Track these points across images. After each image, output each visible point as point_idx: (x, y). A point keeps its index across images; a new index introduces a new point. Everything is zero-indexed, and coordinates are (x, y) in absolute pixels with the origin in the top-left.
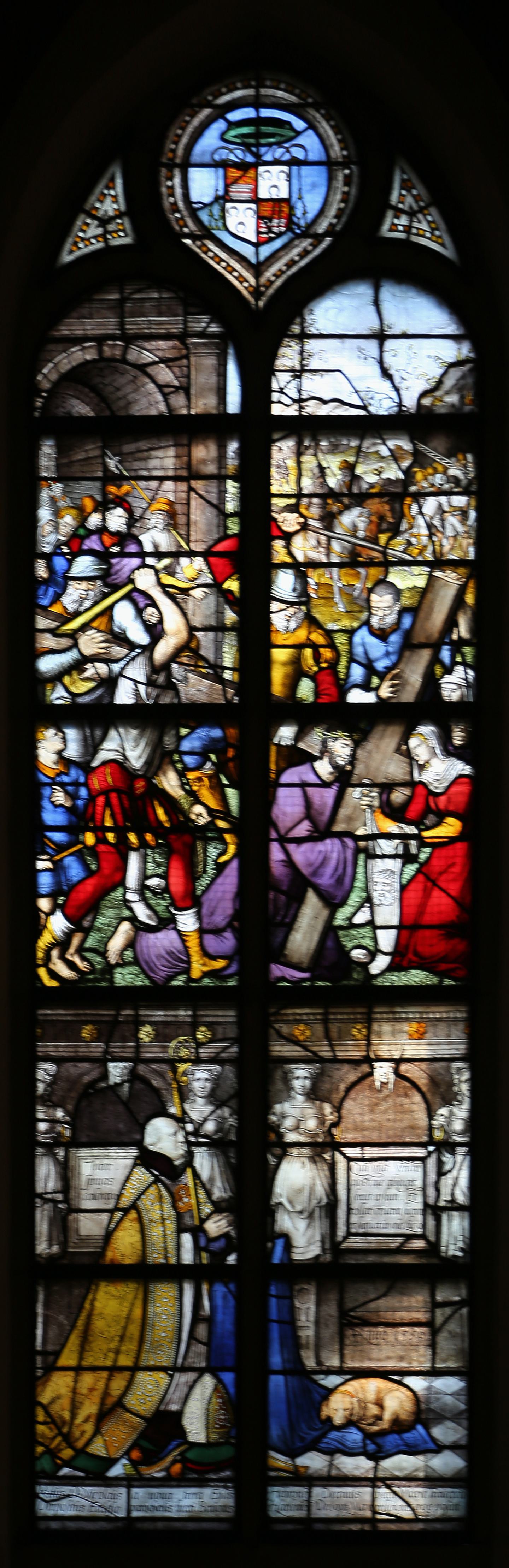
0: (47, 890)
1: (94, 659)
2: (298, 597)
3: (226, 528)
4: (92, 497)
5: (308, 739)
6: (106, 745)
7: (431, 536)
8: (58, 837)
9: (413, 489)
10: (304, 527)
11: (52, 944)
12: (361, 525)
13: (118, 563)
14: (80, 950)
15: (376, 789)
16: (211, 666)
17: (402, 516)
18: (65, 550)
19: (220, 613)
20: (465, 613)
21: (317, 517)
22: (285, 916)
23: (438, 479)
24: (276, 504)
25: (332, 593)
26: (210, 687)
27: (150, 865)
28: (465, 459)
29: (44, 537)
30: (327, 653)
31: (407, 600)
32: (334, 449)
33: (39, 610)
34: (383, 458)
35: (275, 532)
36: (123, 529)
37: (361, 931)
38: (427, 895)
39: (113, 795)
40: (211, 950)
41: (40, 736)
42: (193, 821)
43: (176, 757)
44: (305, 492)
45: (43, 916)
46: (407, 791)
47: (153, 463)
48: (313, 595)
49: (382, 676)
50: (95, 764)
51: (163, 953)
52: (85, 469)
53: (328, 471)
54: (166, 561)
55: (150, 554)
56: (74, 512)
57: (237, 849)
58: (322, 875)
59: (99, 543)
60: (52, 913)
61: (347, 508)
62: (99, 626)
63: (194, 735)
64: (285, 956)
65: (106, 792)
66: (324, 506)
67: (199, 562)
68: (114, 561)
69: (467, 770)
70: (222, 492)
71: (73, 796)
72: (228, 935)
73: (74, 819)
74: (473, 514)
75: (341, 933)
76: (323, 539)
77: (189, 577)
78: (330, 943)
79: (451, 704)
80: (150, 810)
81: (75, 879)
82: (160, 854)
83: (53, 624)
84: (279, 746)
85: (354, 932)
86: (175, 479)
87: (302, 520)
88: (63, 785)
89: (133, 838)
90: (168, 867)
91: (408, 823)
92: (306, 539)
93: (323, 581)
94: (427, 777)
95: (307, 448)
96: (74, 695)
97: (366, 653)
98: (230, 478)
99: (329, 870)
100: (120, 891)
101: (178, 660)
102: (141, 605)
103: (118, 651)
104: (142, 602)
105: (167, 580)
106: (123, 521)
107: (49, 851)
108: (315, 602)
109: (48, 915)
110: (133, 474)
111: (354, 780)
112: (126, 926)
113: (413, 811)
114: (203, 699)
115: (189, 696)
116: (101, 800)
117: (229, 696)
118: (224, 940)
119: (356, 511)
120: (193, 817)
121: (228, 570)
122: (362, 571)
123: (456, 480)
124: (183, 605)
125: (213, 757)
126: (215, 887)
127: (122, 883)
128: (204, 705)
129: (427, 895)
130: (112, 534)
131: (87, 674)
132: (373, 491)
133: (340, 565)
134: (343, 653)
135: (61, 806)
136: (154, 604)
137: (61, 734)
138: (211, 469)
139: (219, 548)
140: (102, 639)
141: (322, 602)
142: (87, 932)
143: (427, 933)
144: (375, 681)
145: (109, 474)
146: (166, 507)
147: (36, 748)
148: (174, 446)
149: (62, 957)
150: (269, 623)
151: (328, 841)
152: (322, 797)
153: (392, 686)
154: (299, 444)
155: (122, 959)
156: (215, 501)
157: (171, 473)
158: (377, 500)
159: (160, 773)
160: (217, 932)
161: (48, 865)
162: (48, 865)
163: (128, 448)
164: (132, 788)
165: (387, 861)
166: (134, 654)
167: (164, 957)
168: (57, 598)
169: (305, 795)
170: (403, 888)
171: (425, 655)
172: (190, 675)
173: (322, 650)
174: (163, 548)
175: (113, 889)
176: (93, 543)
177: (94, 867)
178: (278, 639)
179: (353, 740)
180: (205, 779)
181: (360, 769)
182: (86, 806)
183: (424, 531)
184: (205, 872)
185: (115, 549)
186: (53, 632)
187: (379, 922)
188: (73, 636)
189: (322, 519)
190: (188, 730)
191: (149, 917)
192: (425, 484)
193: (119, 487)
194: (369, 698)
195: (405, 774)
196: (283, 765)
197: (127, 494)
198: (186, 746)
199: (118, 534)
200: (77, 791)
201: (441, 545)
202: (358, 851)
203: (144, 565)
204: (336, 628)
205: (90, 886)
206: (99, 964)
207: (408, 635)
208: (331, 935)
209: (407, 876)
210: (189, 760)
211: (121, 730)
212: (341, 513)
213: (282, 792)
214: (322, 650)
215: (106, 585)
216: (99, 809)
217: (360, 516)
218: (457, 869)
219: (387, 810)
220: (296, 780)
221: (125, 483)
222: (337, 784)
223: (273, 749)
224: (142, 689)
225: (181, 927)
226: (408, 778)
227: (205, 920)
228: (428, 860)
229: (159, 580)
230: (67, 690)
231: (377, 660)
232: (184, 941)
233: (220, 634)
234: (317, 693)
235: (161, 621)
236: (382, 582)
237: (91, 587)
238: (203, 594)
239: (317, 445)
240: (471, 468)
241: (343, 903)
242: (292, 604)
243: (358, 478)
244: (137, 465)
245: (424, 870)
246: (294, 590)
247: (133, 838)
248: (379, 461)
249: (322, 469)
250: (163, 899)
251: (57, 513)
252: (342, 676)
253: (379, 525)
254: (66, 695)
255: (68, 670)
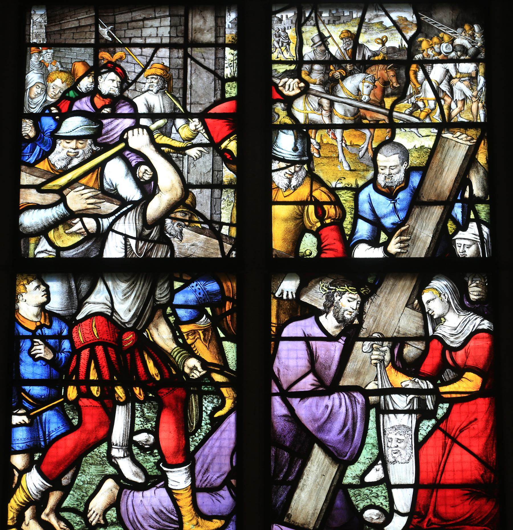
0: (21, 445)
1: (81, 215)
2: (299, 156)
3: (223, 91)
4: (84, 62)
5: (312, 293)
6: (92, 298)
7: (438, 100)
8: (36, 391)
9: (418, 57)
10: (305, 91)
11: (25, 503)
12: (365, 91)
13: (109, 124)
14: (58, 510)
15: (386, 343)
16: (206, 221)
17: (408, 81)
18: (54, 110)
19: (215, 171)
20: (478, 172)
21: (318, 83)
22: (288, 474)
23: (445, 48)
24: (276, 70)
25: (336, 152)
26: (206, 242)
27: (137, 421)
28: (472, 29)
29: (32, 99)
30: (331, 210)
31: (415, 160)
32: (335, 20)
33: (23, 167)
34: (386, 28)
35: (276, 96)
36: (116, 92)
37: (374, 490)
38: (446, 453)
39: (99, 350)
40: (205, 509)
41: (20, 288)
42: (187, 375)
43: (169, 310)
44: (306, 58)
45: (16, 473)
46: (421, 346)
47: (147, 32)
48: (316, 155)
49: (390, 234)
50: (79, 317)
51: (151, 512)
52: (77, 36)
53: (330, 40)
54: (161, 122)
55: (144, 116)
56: (64, 76)
57: (233, 403)
58: (330, 431)
59: (89, 104)
60: (27, 469)
61: (351, 73)
62: (88, 183)
63: (189, 289)
64: (289, 516)
65: (91, 346)
66: (326, 71)
67: (195, 123)
68: (105, 122)
69: (486, 325)
70: (220, 60)
71: (56, 350)
72: (225, 493)
73: (54, 372)
74: (481, 80)
75: (351, 492)
76: (325, 103)
77: (183, 136)
78: (338, 502)
79: (465, 259)
80: (139, 363)
81: (54, 435)
82: (150, 409)
83: (40, 181)
84: (280, 299)
85: (365, 491)
86: (171, 46)
87: (302, 85)
88: (44, 338)
89: (119, 391)
90: (158, 422)
91: (424, 378)
92: (306, 102)
93: (325, 141)
94: (443, 331)
95: (307, 19)
96: (59, 249)
97: (373, 209)
98: (229, 46)
99: (337, 425)
100: (104, 447)
101: (173, 215)
102: (133, 163)
103: (108, 207)
104: (134, 160)
105: (161, 140)
106: (115, 84)
107: (27, 405)
108: (316, 161)
109: (22, 473)
110: (127, 41)
111: (363, 334)
112: (110, 483)
113: (428, 366)
114: (198, 253)
115: (183, 251)
116: (85, 354)
117: (227, 251)
118: (219, 498)
119: (360, 77)
120: (187, 370)
121: (226, 131)
122: (367, 132)
123: (464, 50)
124: (178, 163)
125: (208, 309)
126: (210, 443)
127: (108, 438)
128: (199, 260)
129: (446, 453)
130: (104, 97)
131: (74, 229)
132: (376, 58)
133: (344, 127)
134: (348, 210)
135: (40, 358)
136: (147, 162)
137: (43, 288)
138: (209, 37)
139: (217, 110)
140: (90, 194)
141: (325, 161)
142: (66, 491)
143: (449, 492)
144: (383, 237)
145: (102, 41)
146: (159, 72)
147: (16, 301)
148: (170, 16)
149: (37, 517)
150: (270, 180)
151: (336, 395)
152: (328, 350)
153: (401, 242)
154: (299, 16)
155: (104, 519)
156: (212, 67)
157: (166, 41)
158: (381, 66)
159: (151, 326)
160: (212, 490)
161: (25, 419)
162: (25, 419)
163: (120, 18)
164: (120, 340)
165: (400, 416)
166: (125, 209)
167: (151, 517)
168: (45, 155)
169: (309, 348)
170: (418, 446)
171: (437, 211)
172: (185, 230)
173: (326, 207)
174: (157, 110)
175: (98, 444)
176: (84, 105)
177: (75, 422)
178: (279, 196)
179: (359, 293)
180: (200, 332)
181: (368, 323)
182: (69, 360)
183: (431, 95)
184: (199, 426)
185: (106, 111)
186: (39, 188)
187: (394, 480)
188: (60, 191)
189: (323, 84)
190: (182, 284)
191: (136, 474)
192: (430, 52)
193: (113, 53)
194: (378, 253)
195: (417, 329)
196: (284, 318)
197: (121, 59)
198: (179, 299)
199: (109, 96)
200: (60, 345)
201: (450, 108)
202: (368, 406)
203: (137, 125)
204: (339, 186)
205: (71, 440)
206: (77, 524)
207: (416, 193)
208: (340, 492)
209: (423, 432)
210: (182, 313)
211: (110, 284)
212: (343, 78)
213: (283, 345)
214: (326, 207)
215: (96, 144)
216: (83, 362)
217: (364, 80)
218: (480, 425)
219: (399, 364)
220: (300, 334)
221: (117, 49)
222: (344, 338)
223: (274, 303)
224: (133, 242)
225: (171, 485)
226: (421, 331)
227: (199, 478)
228: (446, 416)
229: (152, 141)
230: (51, 243)
231: (385, 216)
232: (174, 501)
233: (217, 192)
234: (320, 248)
235: (155, 177)
236: (390, 141)
237: (80, 146)
238: (199, 153)
239: (318, 17)
240: (478, 37)
241: (354, 459)
242: (293, 163)
243: (362, 46)
244: (130, 33)
245: (442, 426)
246: (295, 149)
247: (119, 391)
248: (381, 31)
249: (323, 40)
250: (152, 454)
251: (46, 76)
252: (347, 232)
253: (384, 90)
254: (50, 248)
255: (54, 225)
